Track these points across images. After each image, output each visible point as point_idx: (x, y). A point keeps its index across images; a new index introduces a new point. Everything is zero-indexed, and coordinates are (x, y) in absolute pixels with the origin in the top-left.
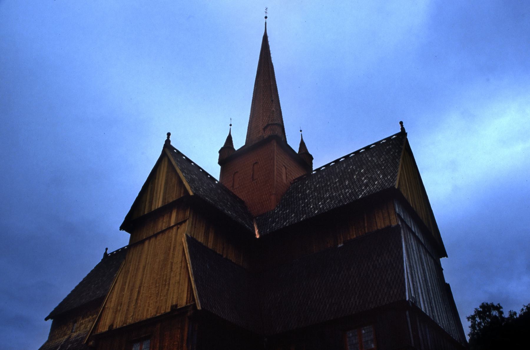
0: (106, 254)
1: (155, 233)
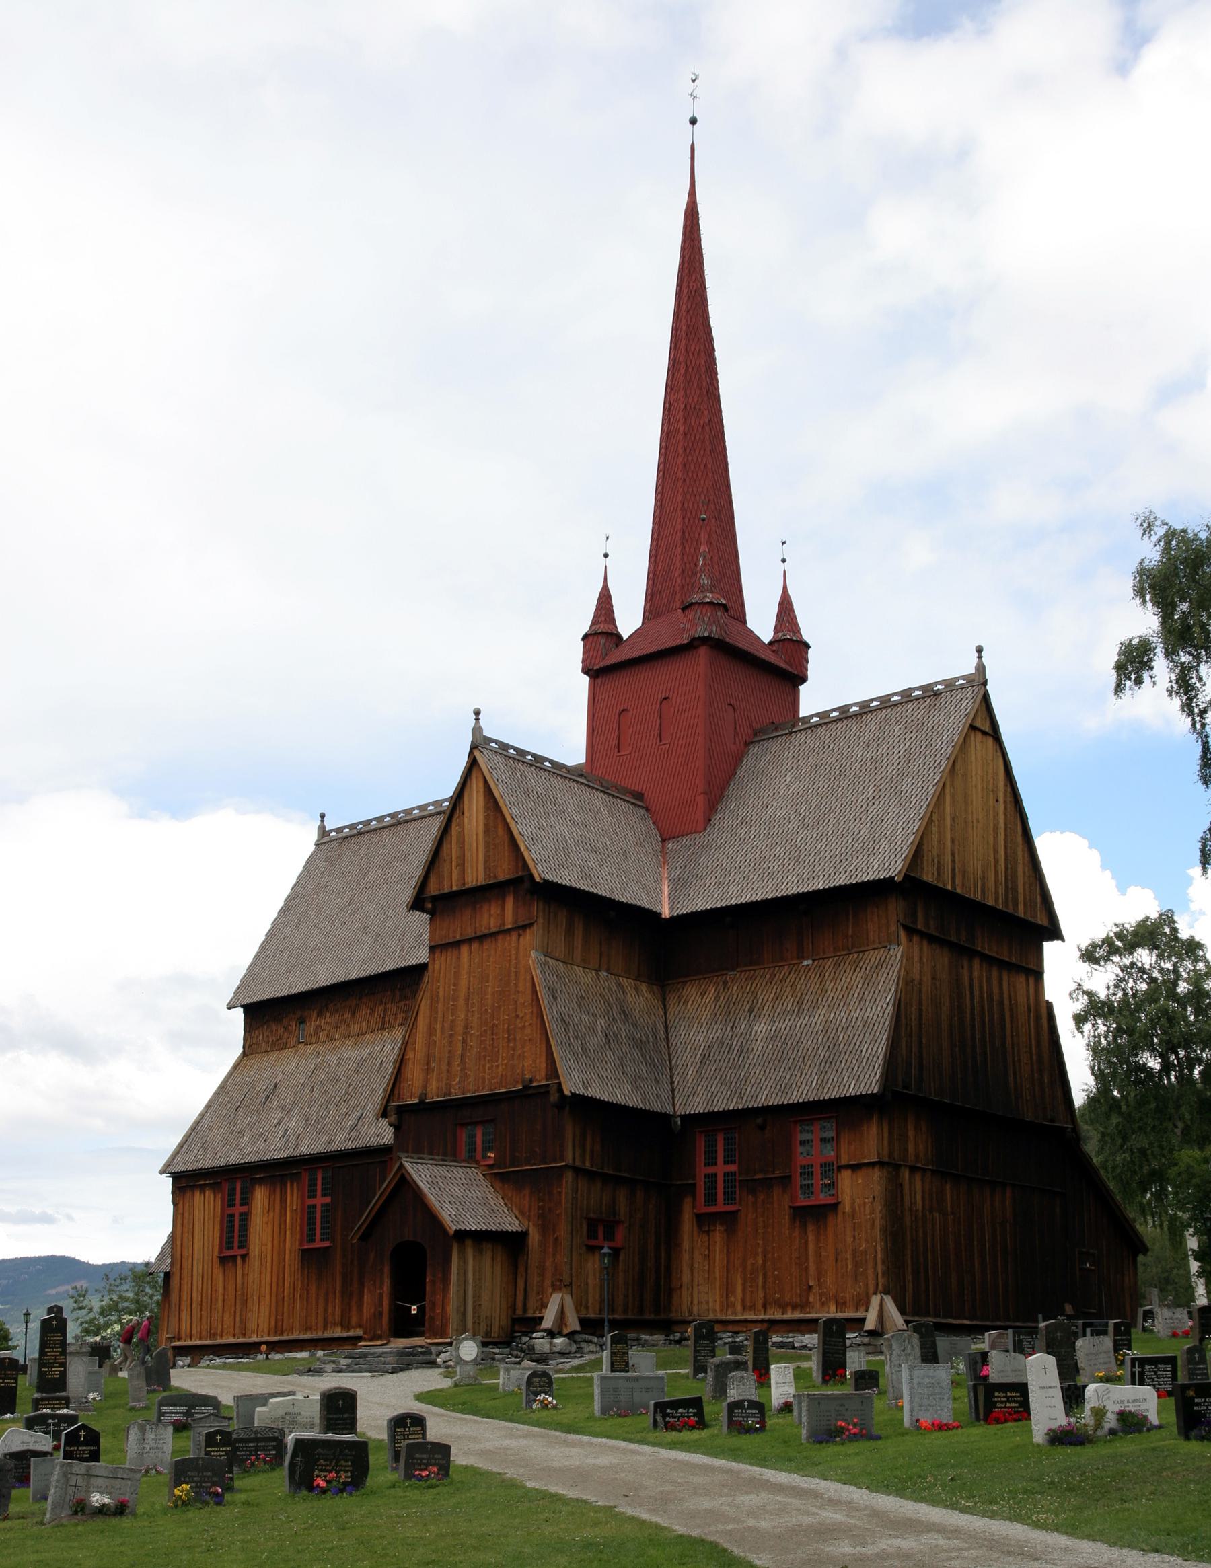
0: (323, 832)
1: (479, 934)
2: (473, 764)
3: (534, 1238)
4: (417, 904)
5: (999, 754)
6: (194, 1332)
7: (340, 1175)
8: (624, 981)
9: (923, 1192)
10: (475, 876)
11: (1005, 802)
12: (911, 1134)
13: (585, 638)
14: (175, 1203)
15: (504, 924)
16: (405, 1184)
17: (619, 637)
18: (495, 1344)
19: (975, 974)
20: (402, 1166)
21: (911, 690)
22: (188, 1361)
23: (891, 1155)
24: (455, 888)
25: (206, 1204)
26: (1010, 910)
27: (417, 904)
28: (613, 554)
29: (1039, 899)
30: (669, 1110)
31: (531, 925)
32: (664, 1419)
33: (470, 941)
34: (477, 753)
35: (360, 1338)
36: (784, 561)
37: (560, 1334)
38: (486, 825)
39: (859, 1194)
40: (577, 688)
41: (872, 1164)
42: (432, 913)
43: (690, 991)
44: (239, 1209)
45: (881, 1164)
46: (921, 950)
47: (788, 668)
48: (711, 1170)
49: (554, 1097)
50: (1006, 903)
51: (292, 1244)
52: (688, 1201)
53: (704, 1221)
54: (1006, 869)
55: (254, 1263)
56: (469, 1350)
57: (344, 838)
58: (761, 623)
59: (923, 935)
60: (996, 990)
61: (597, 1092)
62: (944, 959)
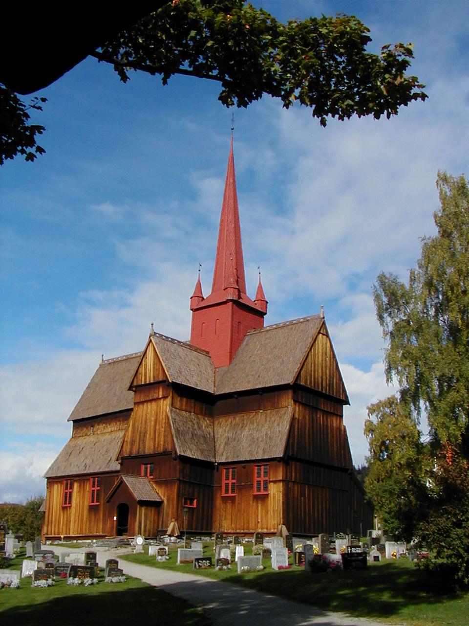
2: (151, 341)
4: (130, 389)
6: (53, 532)
7: (102, 478)
8: (200, 416)
13: (191, 298)
15: (159, 396)
16: (122, 482)
17: (203, 299)
18: (151, 539)
19: (318, 416)
20: (121, 478)
22: (50, 542)
24: (143, 383)
25: (58, 490)
27: (130, 389)
30: (213, 460)
31: (168, 397)
32: (198, 563)
33: (147, 401)
34: (151, 338)
35: (106, 536)
36: (260, 273)
37: (173, 536)
38: (154, 362)
39: (276, 492)
40: (188, 316)
42: (135, 392)
43: (222, 420)
44: (69, 491)
47: (260, 310)
48: (227, 482)
49: (174, 456)
50: (329, 392)
51: (87, 503)
52: (219, 492)
53: (225, 499)
55: (73, 509)
56: (140, 540)
57: (110, 364)
58: (251, 294)
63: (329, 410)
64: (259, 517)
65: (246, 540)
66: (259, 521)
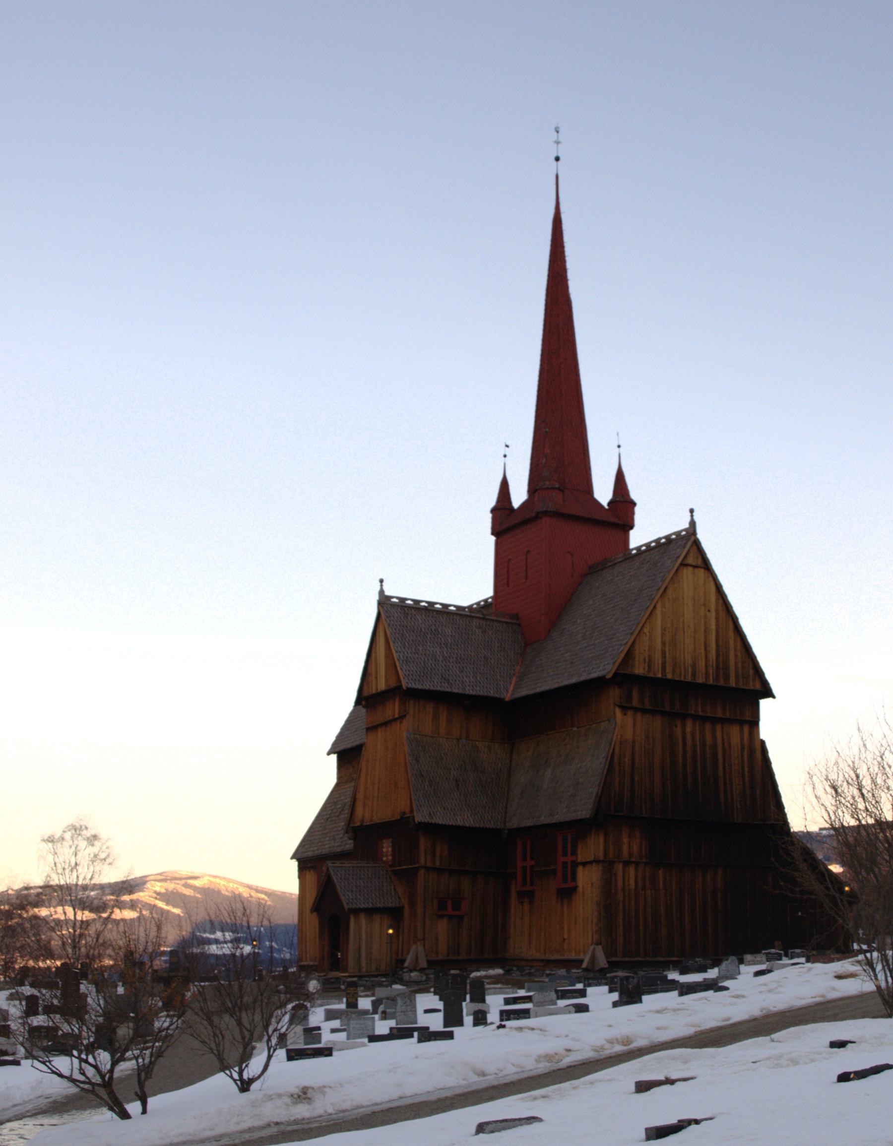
3: (407, 910)
5: (711, 579)
9: (636, 877)
10: (382, 686)
11: (717, 611)
12: (625, 840)
13: (493, 511)
14: (300, 877)
18: (383, 975)
19: (688, 729)
21: (660, 539)
23: (606, 854)
24: (374, 692)
26: (722, 682)
28: (508, 456)
29: (751, 672)
30: (499, 826)
31: (405, 716)
36: (619, 446)
37: (415, 970)
41: (591, 863)
45: (596, 861)
46: (635, 720)
53: (521, 895)
54: (718, 656)
59: (635, 710)
60: (709, 739)
61: (439, 820)
62: (657, 723)
63: (720, 714)
64: (566, 929)
65: (548, 972)
66: (566, 936)
